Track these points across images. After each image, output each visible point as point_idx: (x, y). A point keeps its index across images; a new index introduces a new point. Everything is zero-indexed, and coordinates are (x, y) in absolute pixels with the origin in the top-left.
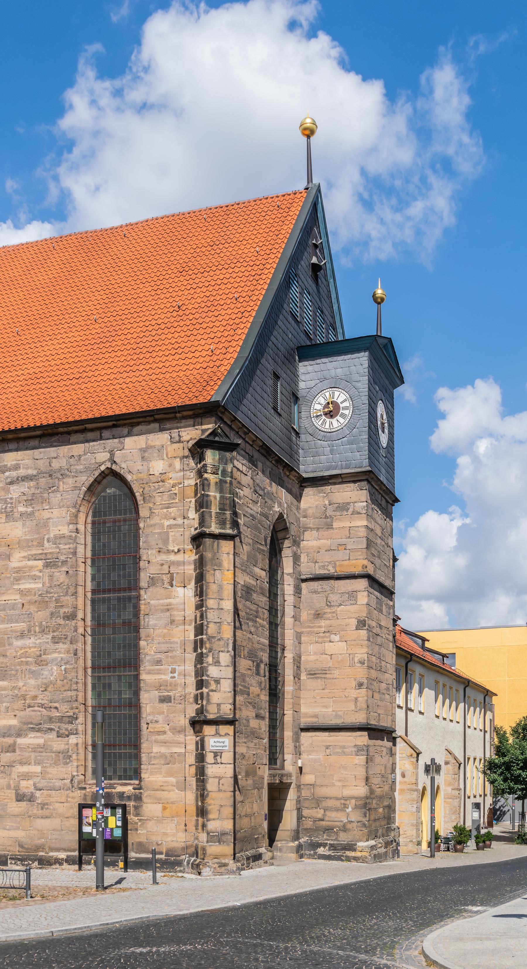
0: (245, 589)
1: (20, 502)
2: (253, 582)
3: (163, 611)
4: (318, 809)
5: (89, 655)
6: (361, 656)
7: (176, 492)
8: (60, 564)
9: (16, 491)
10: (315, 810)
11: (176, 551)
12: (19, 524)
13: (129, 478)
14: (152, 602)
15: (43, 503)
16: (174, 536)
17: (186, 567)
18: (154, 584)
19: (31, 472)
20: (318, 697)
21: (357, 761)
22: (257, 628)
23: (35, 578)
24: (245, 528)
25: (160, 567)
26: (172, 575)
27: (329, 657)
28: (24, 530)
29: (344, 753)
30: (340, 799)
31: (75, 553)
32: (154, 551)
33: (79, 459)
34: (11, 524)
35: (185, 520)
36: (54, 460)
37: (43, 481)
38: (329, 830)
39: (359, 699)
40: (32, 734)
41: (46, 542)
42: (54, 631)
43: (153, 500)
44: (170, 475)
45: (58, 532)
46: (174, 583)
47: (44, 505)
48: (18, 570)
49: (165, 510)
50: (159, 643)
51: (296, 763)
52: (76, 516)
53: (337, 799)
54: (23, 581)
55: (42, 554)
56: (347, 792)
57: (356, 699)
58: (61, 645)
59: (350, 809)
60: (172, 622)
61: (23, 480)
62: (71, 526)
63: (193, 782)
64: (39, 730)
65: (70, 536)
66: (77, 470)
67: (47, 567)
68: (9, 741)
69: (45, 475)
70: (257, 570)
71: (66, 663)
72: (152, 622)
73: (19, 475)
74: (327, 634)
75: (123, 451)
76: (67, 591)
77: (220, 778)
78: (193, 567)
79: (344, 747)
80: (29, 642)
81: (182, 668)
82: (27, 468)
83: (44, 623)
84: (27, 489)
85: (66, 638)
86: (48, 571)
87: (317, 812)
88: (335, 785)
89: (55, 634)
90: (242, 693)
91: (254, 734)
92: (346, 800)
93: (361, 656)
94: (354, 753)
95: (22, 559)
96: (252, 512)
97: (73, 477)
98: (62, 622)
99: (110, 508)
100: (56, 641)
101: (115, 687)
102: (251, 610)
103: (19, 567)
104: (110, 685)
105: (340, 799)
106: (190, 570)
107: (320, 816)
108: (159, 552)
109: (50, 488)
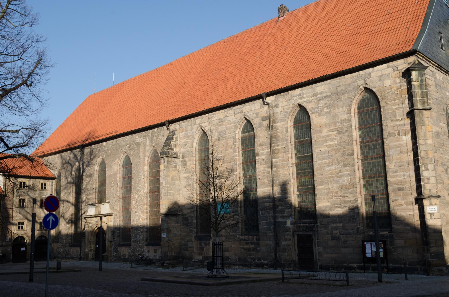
2: (440, 130)
3: (396, 148)
5: (361, 171)
7: (398, 93)
9: (322, 103)
13: (374, 90)
14: (390, 144)
17: (406, 126)
18: (390, 136)
19: (328, 94)
22: (444, 151)
23: (333, 139)
24: (433, 105)
26: (399, 131)
31: (351, 126)
32: (389, 121)
35: (404, 105)
37: (334, 97)
42: (344, 162)
45: (342, 118)
46: (401, 134)
48: (326, 136)
49: (393, 102)
52: (350, 110)
58: (347, 168)
60: (401, 152)
62: (348, 115)
64: (340, 207)
66: (349, 90)
71: (350, 176)
78: (409, 126)
80: (333, 167)
81: (408, 173)
82: (326, 93)
86: (339, 136)
90: (440, 183)
96: (436, 97)
98: (347, 157)
99: (366, 104)
100: (345, 166)
104: (372, 184)
106: (408, 127)
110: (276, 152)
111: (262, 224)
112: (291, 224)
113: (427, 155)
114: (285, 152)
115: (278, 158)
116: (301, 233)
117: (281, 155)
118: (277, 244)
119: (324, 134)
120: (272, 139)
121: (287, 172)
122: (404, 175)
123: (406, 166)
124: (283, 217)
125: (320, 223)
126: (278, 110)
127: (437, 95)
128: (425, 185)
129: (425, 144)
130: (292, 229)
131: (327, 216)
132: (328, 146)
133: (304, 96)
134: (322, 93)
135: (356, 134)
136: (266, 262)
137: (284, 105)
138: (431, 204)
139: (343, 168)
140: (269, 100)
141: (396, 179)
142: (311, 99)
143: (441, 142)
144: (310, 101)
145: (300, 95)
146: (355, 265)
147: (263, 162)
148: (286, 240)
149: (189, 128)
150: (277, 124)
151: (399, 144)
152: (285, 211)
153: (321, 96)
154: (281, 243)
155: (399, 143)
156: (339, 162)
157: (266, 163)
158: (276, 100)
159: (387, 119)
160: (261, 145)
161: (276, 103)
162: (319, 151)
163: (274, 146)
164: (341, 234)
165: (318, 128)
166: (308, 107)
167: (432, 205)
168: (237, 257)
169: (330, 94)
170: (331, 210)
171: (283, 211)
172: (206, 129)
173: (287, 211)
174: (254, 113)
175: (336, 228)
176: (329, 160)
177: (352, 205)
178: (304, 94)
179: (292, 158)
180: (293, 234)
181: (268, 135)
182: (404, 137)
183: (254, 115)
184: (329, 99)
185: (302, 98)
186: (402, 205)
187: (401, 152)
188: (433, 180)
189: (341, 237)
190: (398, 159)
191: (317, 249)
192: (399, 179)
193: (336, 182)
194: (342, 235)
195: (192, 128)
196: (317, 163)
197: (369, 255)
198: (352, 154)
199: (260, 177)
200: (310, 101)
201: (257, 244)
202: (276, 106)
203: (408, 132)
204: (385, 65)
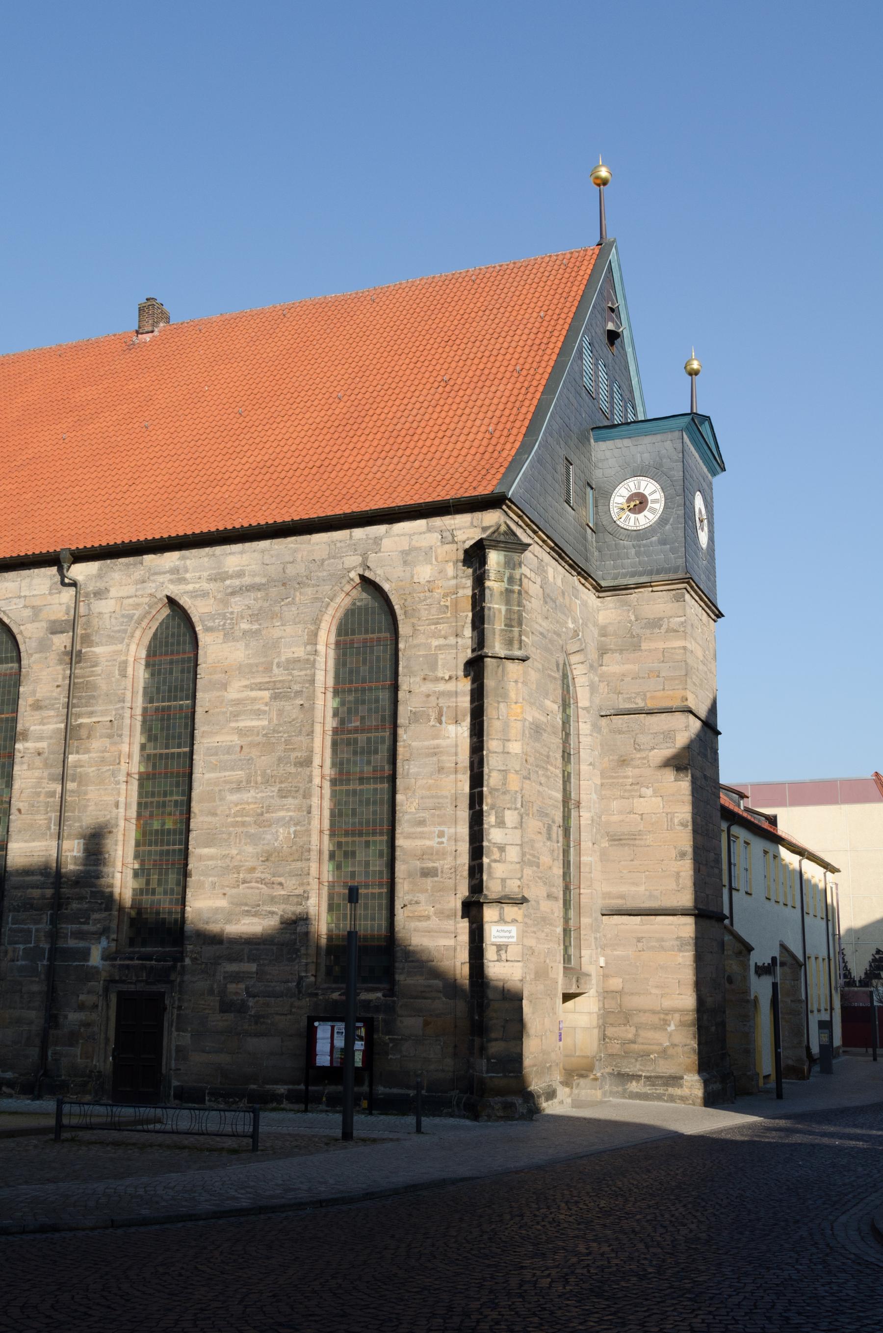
0: (533, 727)
1: (243, 618)
3: (428, 755)
4: (628, 1027)
5: (327, 814)
6: (683, 815)
7: (448, 604)
8: (293, 695)
9: (237, 604)
10: (623, 1028)
11: (447, 678)
12: (241, 645)
13: (386, 587)
14: (414, 744)
15: (272, 618)
16: (445, 659)
17: (459, 699)
18: (417, 721)
19: (257, 580)
20: (625, 872)
21: (680, 960)
22: (548, 777)
23: (258, 713)
24: (534, 649)
25: (425, 699)
26: (441, 709)
27: (639, 818)
28: (247, 652)
29: (662, 948)
30: (659, 1013)
31: (312, 681)
32: (418, 679)
33: (322, 564)
34: (230, 644)
35: (459, 640)
36: (289, 565)
37: (274, 592)
38: (644, 1055)
39: (682, 874)
41: (275, 667)
42: (281, 782)
43: (417, 614)
44: (439, 583)
45: (290, 655)
46: (444, 719)
47: (275, 620)
48: (238, 702)
49: (433, 627)
50: (422, 798)
51: (597, 961)
52: (316, 635)
53: (654, 1012)
54: (243, 717)
55: (269, 682)
56: (667, 1003)
57: (678, 873)
58: (290, 800)
59: (672, 1027)
60: (441, 770)
61: (248, 591)
62: (309, 648)
64: (256, 914)
65: (308, 660)
66: (318, 577)
67: (275, 698)
69: (276, 584)
70: (548, 703)
71: (296, 825)
72: (413, 770)
73: (244, 583)
74: (636, 787)
75: (378, 555)
76: (301, 730)
78: (468, 698)
79: (662, 940)
80: (249, 795)
81: (452, 830)
82: (254, 576)
83: (269, 771)
84: (252, 602)
85: (297, 791)
86: (277, 704)
87: (626, 1031)
88: (651, 993)
89: (283, 786)
90: (531, 864)
91: (545, 920)
92: (667, 1014)
93: (683, 815)
94: (676, 948)
95: (242, 689)
96: (541, 629)
97: (314, 586)
98: (293, 770)
99: (360, 624)
100: (283, 794)
102: (542, 754)
103: (238, 699)
104: (353, 854)
105: (659, 1013)
106: (465, 702)
107: (630, 1036)
108: (425, 679)
109: (283, 600)
110: (84, 733)
111: (10, 955)
112: (104, 958)
113: (504, 784)
114: (110, 736)
115: (87, 751)
116: (132, 988)
117: (96, 744)
118: (52, 1019)
119: (233, 693)
120: (76, 692)
121: (110, 799)
122: (441, 834)
123: (450, 810)
124: (80, 935)
125: (194, 960)
126: (104, 607)
128: (494, 865)
129: (503, 753)
130: (104, 975)
131: (216, 940)
132: (241, 732)
133: (188, 576)
134: (240, 574)
135: (325, 706)
136: (9, 1075)
137: (125, 596)
138: (502, 920)
139: (277, 801)
140: (79, 571)
141: (419, 843)
142: (206, 586)
143: (544, 751)
144: (205, 595)
145: (175, 571)
146: (282, 1089)
148: (81, 1007)
150: (97, 650)
151: (438, 747)
152: (89, 918)
153: (237, 582)
154: (66, 1017)
155: (436, 742)
156: (267, 781)
157: (46, 765)
158: (100, 576)
159: (411, 674)
160: (37, 706)
161: (100, 585)
162: (213, 742)
163: (79, 716)
164: (250, 995)
165: (216, 677)
166: (197, 610)
167: (506, 922)
169: (264, 581)
170: (229, 921)
171: (83, 916)
173: (96, 916)
174: (25, 607)
175: (237, 977)
176: (239, 774)
177: (292, 910)
178: (187, 571)
179: (130, 756)
180: (106, 990)
181: (64, 678)
182: (452, 728)
183: (27, 613)
184: (259, 594)
185: (182, 580)
186: (428, 918)
187: (441, 770)
188: (513, 854)
189: (251, 1002)
190: (429, 788)
191: (175, 1039)
192: (428, 843)
193: (253, 839)
194: (254, 996)
196: (204, 776)
197: (323, 1059)
198: (307, 762)
199: (21, 805)
200: (205, 595)
202: (99, 594)
203: (464, 716)
204: (421, 524)
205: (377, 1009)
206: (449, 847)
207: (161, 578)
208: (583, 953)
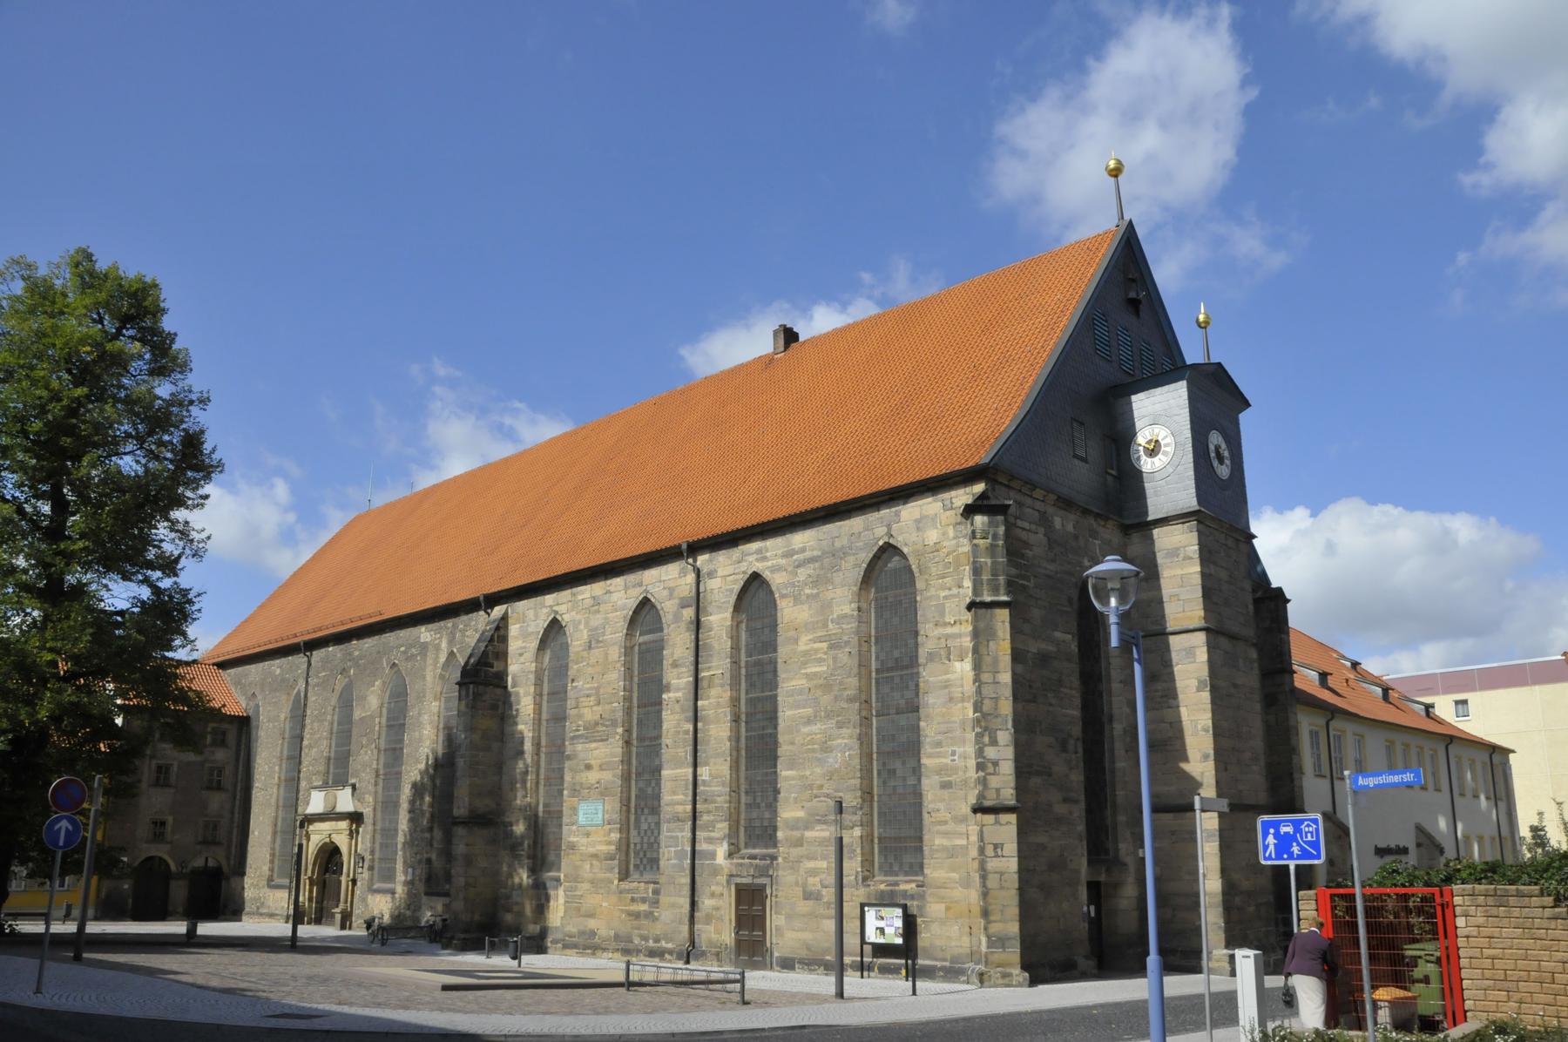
9: (803, 574)
12: (805, 607)
13: (905, 550)
19: (816, 553)
23: (820, 661)
37: (826, 561)
40: (818, 827)
48: (806, 653)
60: (951, 699)
63: (976, 877)
68: (797, 834)
72: (931, 701)
77: (1002, 874)
80: (816, 728)
98: (845, 705)
100: (840, 725)
101: (899, 773)
104: (894, 771)
116: (744, 881)
117: (713, 692)
119: (802, 647)
122: (953, 753)
123: (958, 733)
124: (710, 840)
127: (1052, 567)
130: (726, 871)
132: (809, 677)
134: (803, 550)
136: (670, 946)
137: (725, 572)
145: (759, 551)
147: (677, 708)
148: (713, 895)
149: (531, 614)
153: (801, 557)
156: (828, 716)
157: (683, 711)
158: (711, 560)
160: (675, 665)
161: (712, 567)
162: (792, 685)
165: (792, 633)
166: (777, 580)
168: (612, 933)
172: (566, 619)
173: (719, 825)
175: (813, 872)
180: (728, 882)
182: (957, 665)
183: (666, 593)
185: (764, 559)
186: (945, 823)
187: (951, 699)
195: (536, 616)
196: (786, 714)
199: (669, 741)
201: (656, 903)
202: (711, 574)
205: (912, 897)
206: (959, 762)
207: (751, 558)
208: (1121, 846)
